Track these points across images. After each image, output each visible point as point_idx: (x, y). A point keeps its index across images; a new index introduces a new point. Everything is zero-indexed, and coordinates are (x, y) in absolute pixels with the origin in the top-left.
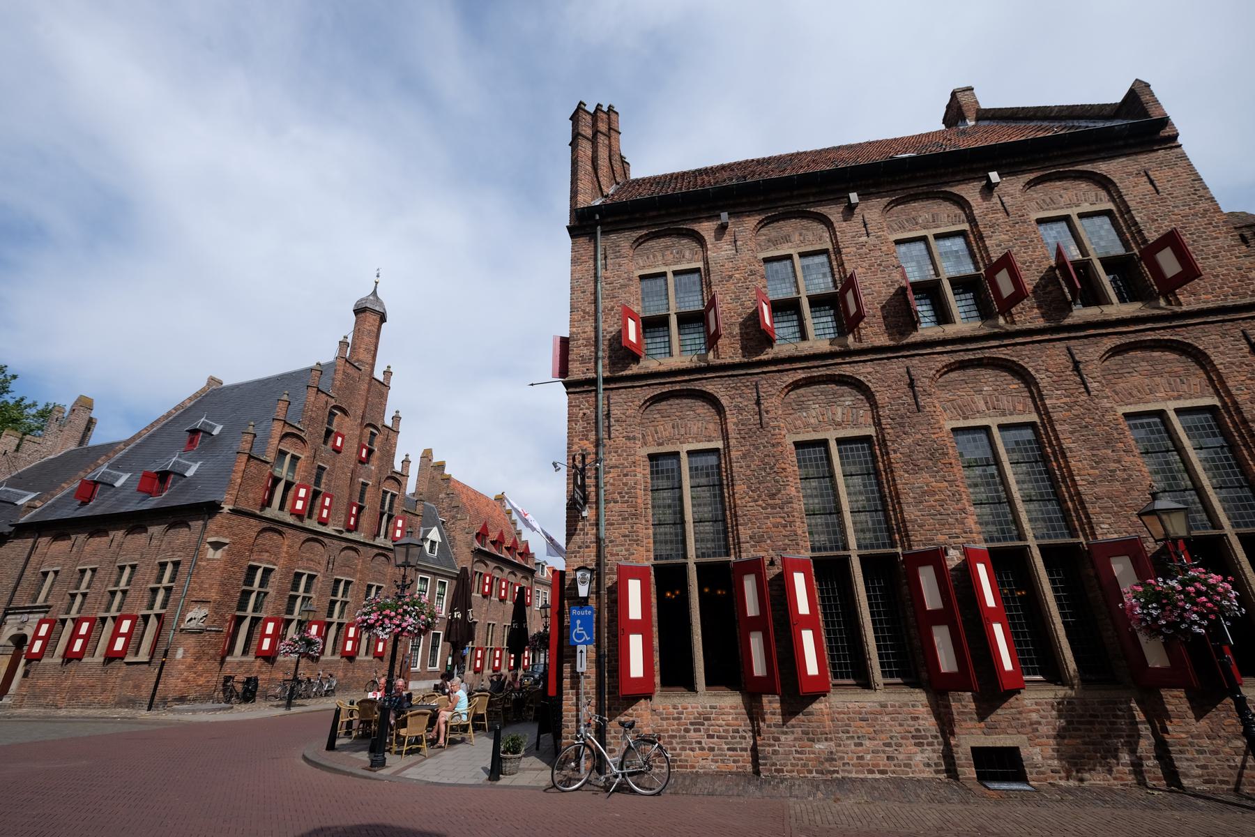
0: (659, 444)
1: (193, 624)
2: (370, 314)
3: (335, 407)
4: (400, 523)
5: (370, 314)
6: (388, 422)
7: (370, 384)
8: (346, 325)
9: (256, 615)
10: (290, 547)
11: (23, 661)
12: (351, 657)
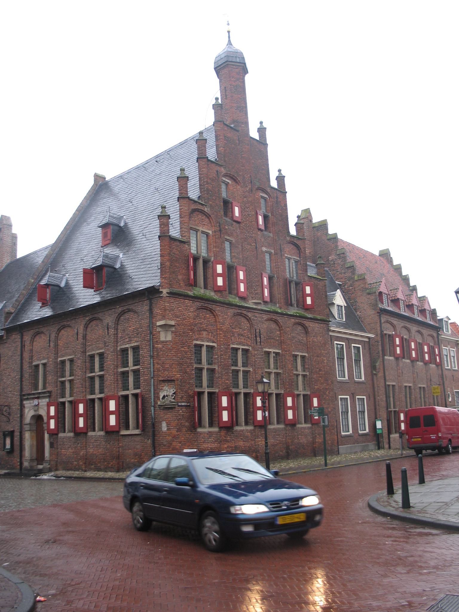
1: (167, 401)
4: (308, 290)
11: (46, 436)
12: (293, 424)
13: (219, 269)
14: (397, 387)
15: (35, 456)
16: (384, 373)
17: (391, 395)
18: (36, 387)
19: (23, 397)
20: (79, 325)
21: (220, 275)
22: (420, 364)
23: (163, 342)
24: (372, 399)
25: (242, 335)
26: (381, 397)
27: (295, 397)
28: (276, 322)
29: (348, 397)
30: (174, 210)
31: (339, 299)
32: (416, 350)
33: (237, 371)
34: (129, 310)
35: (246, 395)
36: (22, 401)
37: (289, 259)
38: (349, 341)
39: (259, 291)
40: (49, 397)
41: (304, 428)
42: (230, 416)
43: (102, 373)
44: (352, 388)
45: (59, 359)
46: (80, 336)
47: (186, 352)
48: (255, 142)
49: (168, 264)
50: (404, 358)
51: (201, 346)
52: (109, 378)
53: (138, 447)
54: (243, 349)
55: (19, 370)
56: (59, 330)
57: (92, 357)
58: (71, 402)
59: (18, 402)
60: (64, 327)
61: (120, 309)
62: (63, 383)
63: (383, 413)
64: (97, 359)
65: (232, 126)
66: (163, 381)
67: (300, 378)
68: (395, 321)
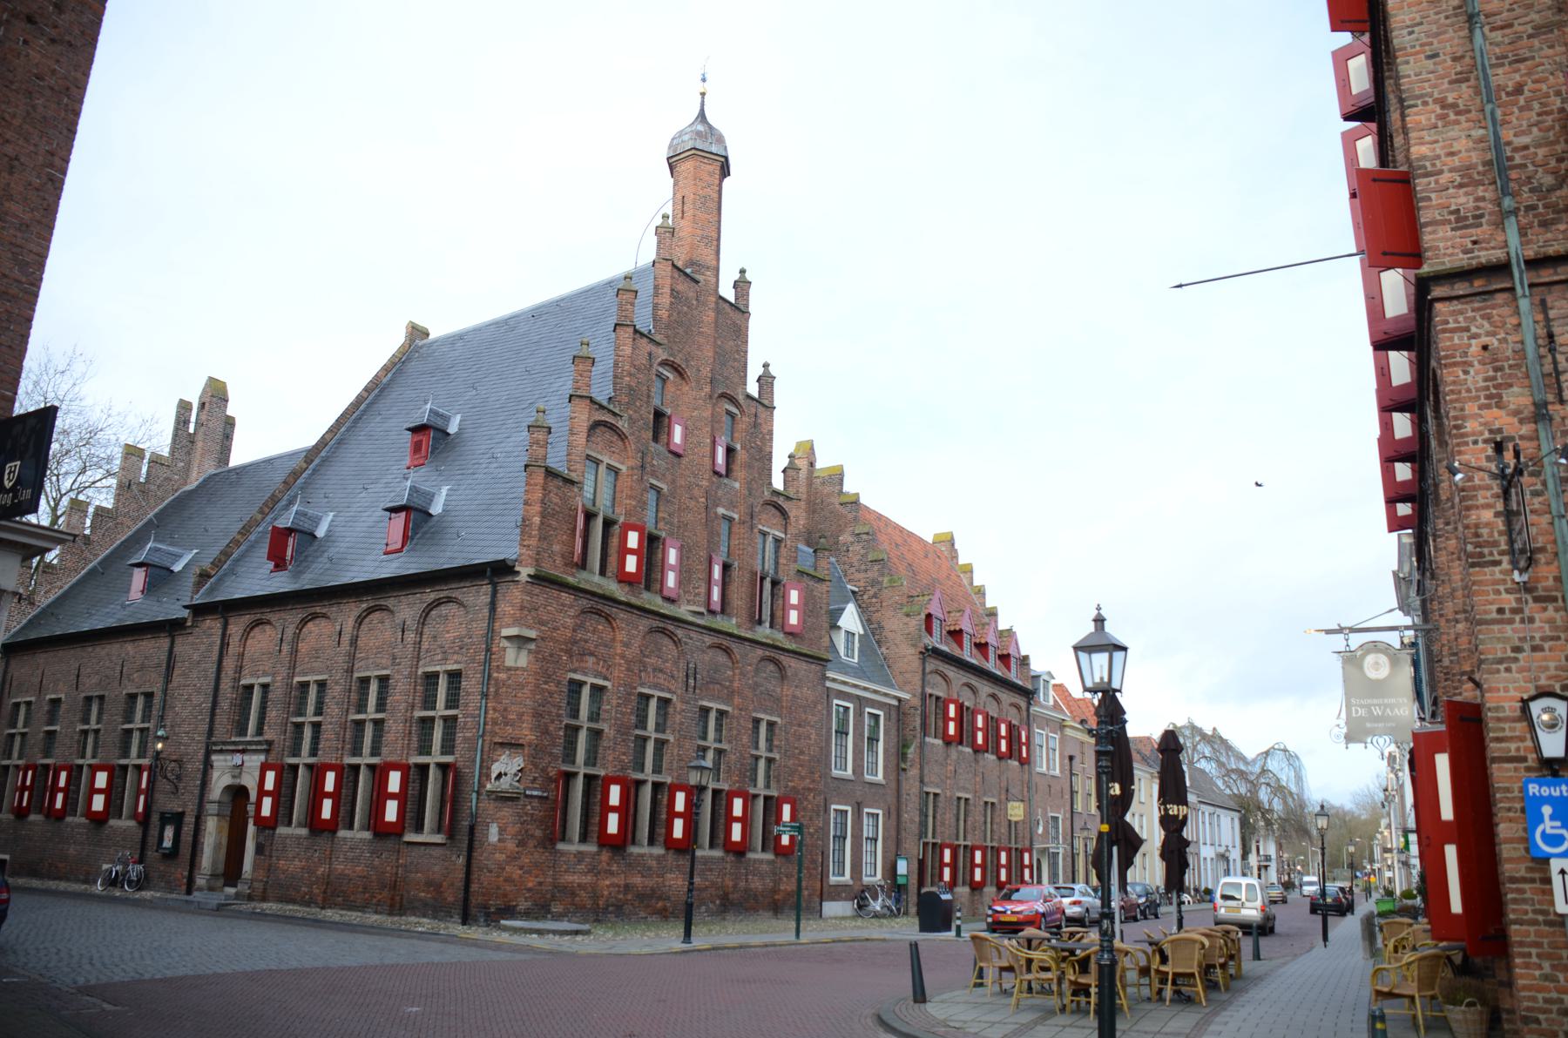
1: (505, 784)
2: (702, 162)
3: (664, 363)
4: (794, 597)
5: (702, 162)
7: (718, 311)
8: (656, 194)
9: (591, 771)
10: (627, 645)
11: (251, 829)
12: (739, 851)
13: (633, 540)
14: (941, 798)
15: (221, 868)
16: (922, 769)
20: (346, 615)
21: (632, 552)
22: (991, 757)
23: (509, 669)
24: (894, 816)
25: (661, 671)
26: (911, 815)
27: (749, 800)
29: (849, 808)
31: (850, 619)
32: (986, 730)
34: (450, 600)
35: (657, 786)
36: (208, 753)
37: (764, 534)
38: (861, 702)
39: (703, 590)
40: (267, 751)
41: (761, 861)
42: (622, 824)
44: (859, 793)
45: (297, 679)
46: (346, 638)
47: (551, 694)
48: (726, 306)
49: (537, 520)
50: (961, 743)
51: (581, 684)
52: (394, 728)
53: (436, 868)
55: (210, 691)
56: (304, 622)
57: (365, 681)
58: (309, 767)
59: (201, 755)
60: (314, 616)
61: (433, 596)
62: (299, 727)
63: (913, 847)
64: (374, 687)
65: (688, 271)
66: (502, 744)
67: (762, 764)
68: (951, 672)
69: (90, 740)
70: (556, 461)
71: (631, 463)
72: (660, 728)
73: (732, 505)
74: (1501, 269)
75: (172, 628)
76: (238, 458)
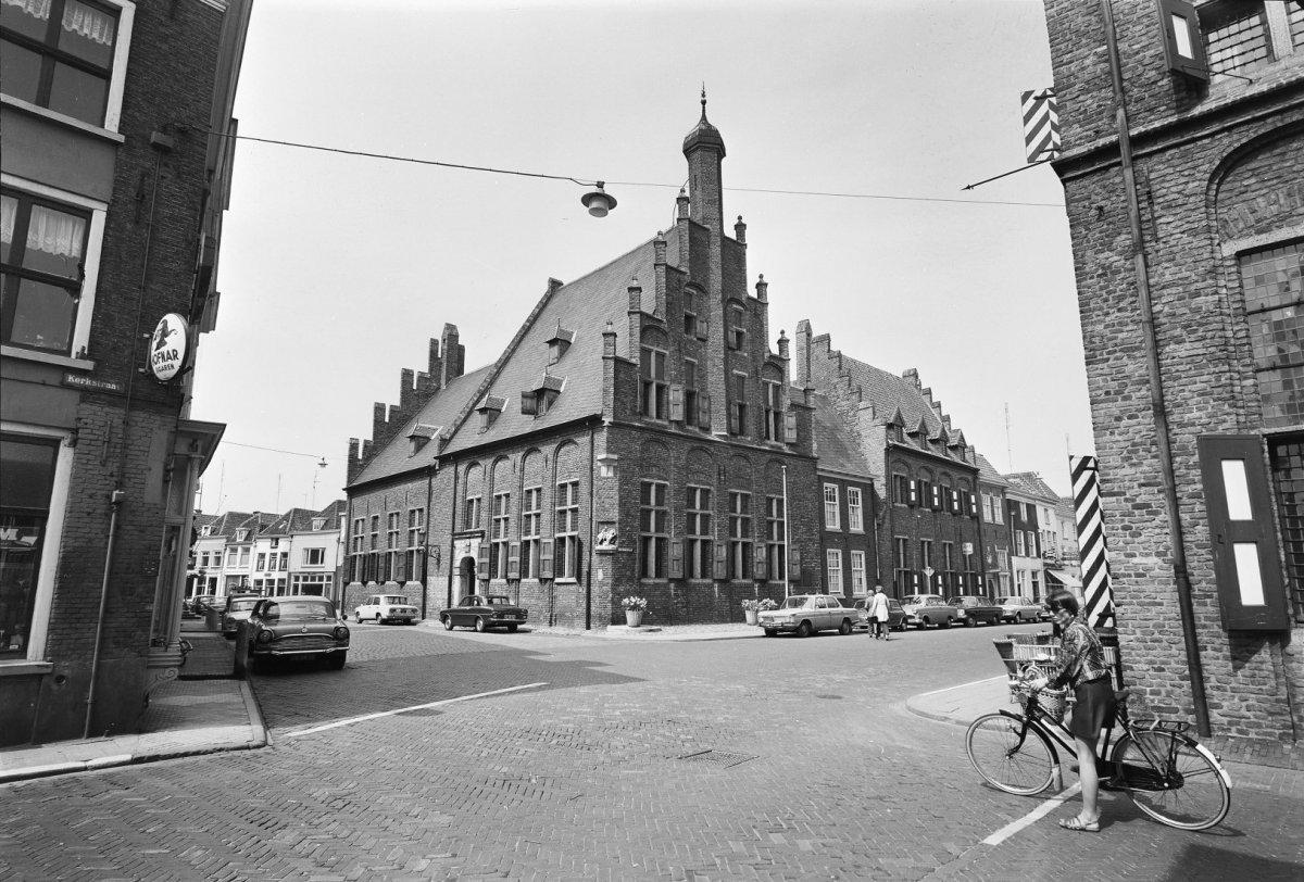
0: (1259, 232)
1: (606, 546)
2: (705, 147)
5: (705, 147)
6: (752, 292)
8: (678, 172)
9: (660, 535)
10: (676, 459)
17: (901, 551)
18: (468, 524)
19: (455, 536)
20: (516, 457)
23: (604, 478)
28: (746, 457)
30: (625, 328)
32: (959, 501)
33: (695, 514)
34: (571, 442)
40: (483, 536)
43: (538, 511)
44: (846, 540)
46: (517, 469)
50: (921, 505)
51: (650, 484)
52: (546, 517)
54: (702, 490)
56: (496, 462)
59: (449, 542)
64: (534, 494)
66: (602, 523)
69: (394, 536)
70: (622, 353)
71: (672, 349)
72: (703, 506)
73: (743, 368)
74: (1113, 149)
75: (427, 472)
76: (467, 370)
